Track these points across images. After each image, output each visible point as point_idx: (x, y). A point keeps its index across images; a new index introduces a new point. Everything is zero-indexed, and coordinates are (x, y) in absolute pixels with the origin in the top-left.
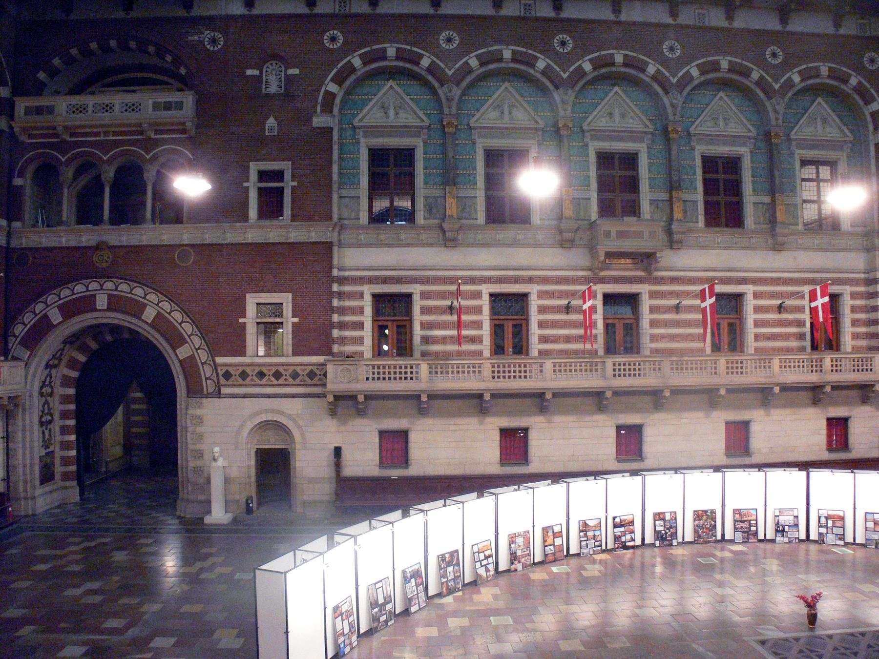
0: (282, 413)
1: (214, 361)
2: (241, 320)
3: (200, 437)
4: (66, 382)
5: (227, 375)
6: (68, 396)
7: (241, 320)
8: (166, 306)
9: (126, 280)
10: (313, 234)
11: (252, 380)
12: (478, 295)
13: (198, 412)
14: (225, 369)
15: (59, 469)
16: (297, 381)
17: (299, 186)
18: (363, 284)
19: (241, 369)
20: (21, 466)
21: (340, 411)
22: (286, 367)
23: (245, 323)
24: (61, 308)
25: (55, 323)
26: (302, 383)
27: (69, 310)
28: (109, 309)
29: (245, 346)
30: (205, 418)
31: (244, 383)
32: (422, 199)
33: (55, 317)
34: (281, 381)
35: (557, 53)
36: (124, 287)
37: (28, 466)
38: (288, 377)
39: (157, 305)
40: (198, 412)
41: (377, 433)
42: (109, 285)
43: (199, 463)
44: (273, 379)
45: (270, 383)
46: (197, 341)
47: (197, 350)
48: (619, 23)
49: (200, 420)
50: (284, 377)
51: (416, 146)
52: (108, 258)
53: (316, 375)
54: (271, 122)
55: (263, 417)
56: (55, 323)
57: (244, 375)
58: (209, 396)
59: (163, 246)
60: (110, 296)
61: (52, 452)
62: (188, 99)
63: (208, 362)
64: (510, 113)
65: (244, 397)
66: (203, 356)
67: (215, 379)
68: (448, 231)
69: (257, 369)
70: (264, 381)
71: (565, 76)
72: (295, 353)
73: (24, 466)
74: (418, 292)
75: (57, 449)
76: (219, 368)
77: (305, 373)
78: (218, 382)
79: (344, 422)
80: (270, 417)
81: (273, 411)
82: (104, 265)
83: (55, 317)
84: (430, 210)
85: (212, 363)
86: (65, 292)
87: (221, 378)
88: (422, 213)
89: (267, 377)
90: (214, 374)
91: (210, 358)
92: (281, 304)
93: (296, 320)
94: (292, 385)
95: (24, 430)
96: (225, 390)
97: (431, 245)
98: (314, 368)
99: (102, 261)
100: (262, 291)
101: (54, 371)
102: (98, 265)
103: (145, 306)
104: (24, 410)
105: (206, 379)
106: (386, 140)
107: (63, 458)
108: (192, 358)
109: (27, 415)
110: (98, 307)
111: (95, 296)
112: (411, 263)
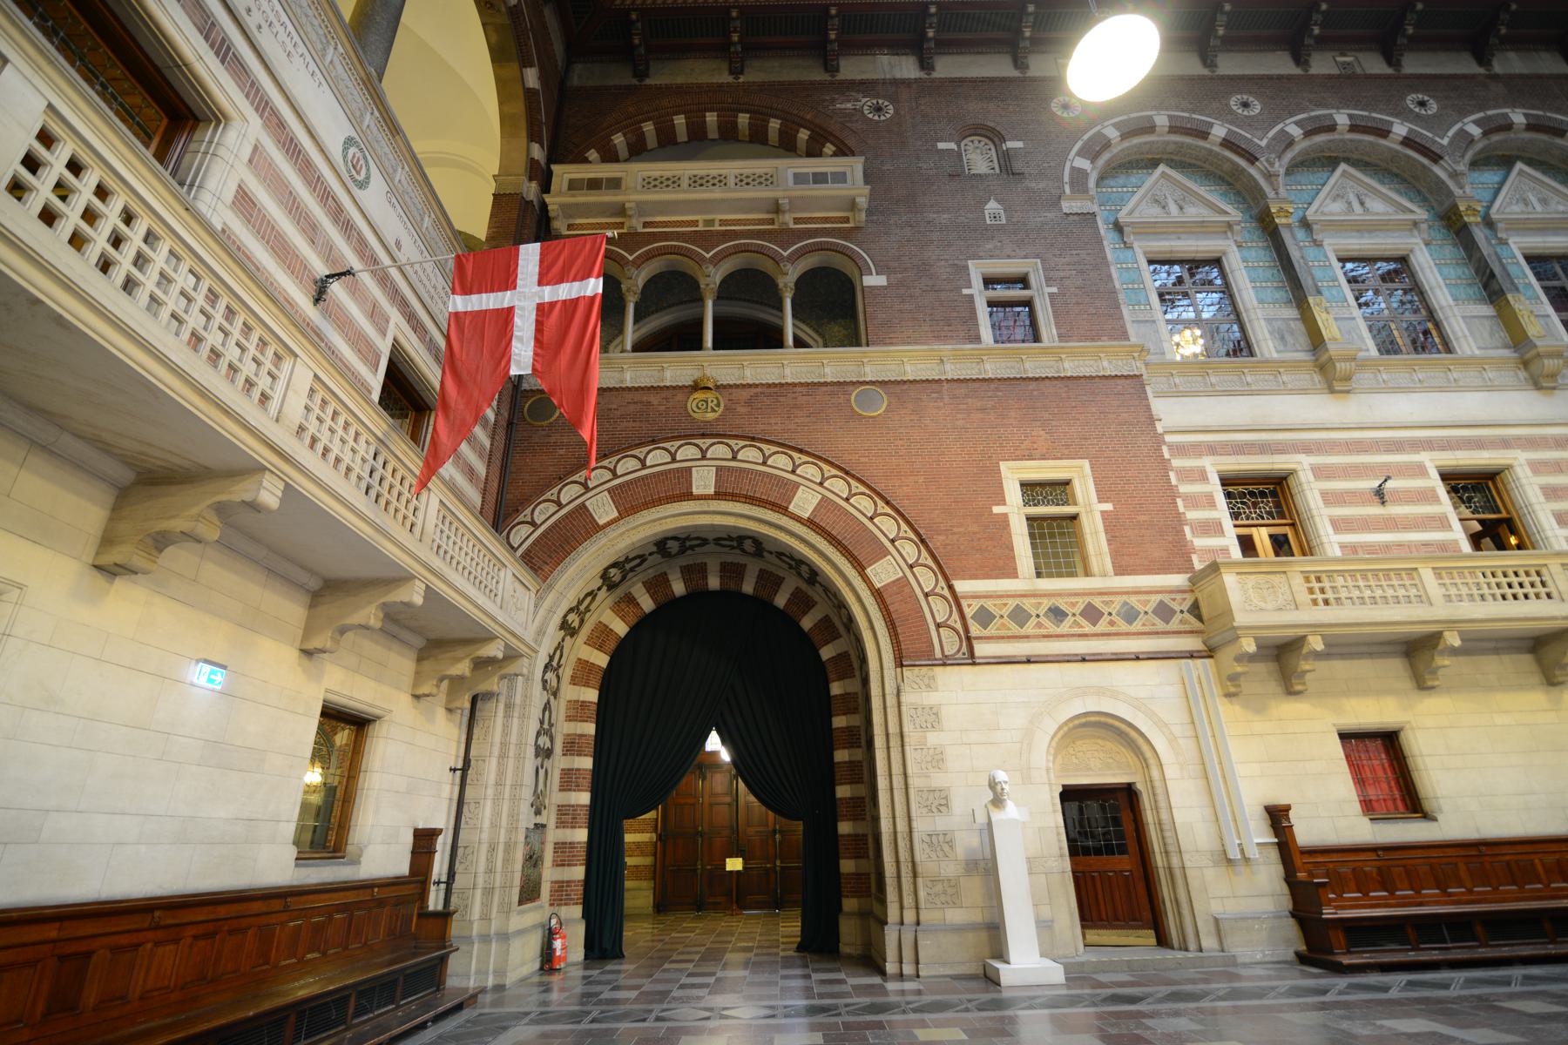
0: (1115, 695)
1: (951, 587)
2: (997, 510)
3: (937, 759)
4: (583, 672)
5: (985, 617)
6: (584, 705)
7: (997, 510)
8: (839, 486)
9: (753, 439)
10: (1105, 363)
11: (1039, 625)
12: (1420, 471)
13: (930, 698)
14: (976, 604)
15: (549, 873)
16: (1137, 626)
17: (1061, 294)
18: (1200, 455)
19: (1012, 603)
20: (484, 848)
21: (1247, 686)
22: (1106, 598)
23: (1005, 515)
24: (616, 493)
25: (601, 522)
26: (1147, 629)
27: (630, 500)
28: (719, 495)
29: (1014, 558)
30: (944, 712)
31: (1023, 632)
32: (1263, 323)
33: (603, 509)
34: (1102, 626)
35: (1418, 116)
36: (750, 454)
37: (501, 848)
38: (1115, 618)
39: (821, 484)
40: (930, 698)
41: (1336, 734)
42: (719, 451)
43: (941, 823)
44: (1084, 622)
45: (1080, 631)
46: (910, 551)
47: (911, 567)
48: (1496, 77)
49: (934, 718)
50: (1106, 618)
51: (1224, 253)
52: (718, 405)
53: (1173, 612)
54: (992, 206)
55: (1078, 707)
56: (601, 522)
57: (1020, 616)
58: (945, 662)
59: (826, 384)
60: (719, 469)
61: (544, 826)
62: (854, 167)
63: (938, 590)
64: (1362, 204)
65: (1029, 662)
66: (927, 579)
67: (959, 626)
68: (1339, 360)
69: (1046, 604)
70: (1065, 627)
71: (1445, 142)
72: (1120, 570)
73: (492, 849)
74: (1306, 466)
75: (552, 824)
76: (964, 603)
77: (1149, 608)
78: (966, 630)
79: (1260, 710)
80: (1092, 705)
81: (1101, 691)
82: (711, 416)
83: (603, 509)
84: (1282, 338)
85: (946, 592)
86: (627, 465)
87: (970, 622)
88: (1271, 344)
89: (1070, 619)
90: (955, 615)
91: (942, 583)
92: (1067, 483)
93: (1108, 507)
94: (1127, 634)
95: (503, 756)
96: (981, 649)
97: (1303, 391)
98: (1166, 598)
99: (705, 409)
100: (1031, 458)
101: (657, 558)
102: (695, 415)
103: (797, 486)
104: (509, 707)
105: (938, 626)
106: (1173, 243)
107: (560, 847)
108: (902, 583)
109: (516, 721)
110: (695, 491)
111: (689, 469)
112: (1276, 421)
